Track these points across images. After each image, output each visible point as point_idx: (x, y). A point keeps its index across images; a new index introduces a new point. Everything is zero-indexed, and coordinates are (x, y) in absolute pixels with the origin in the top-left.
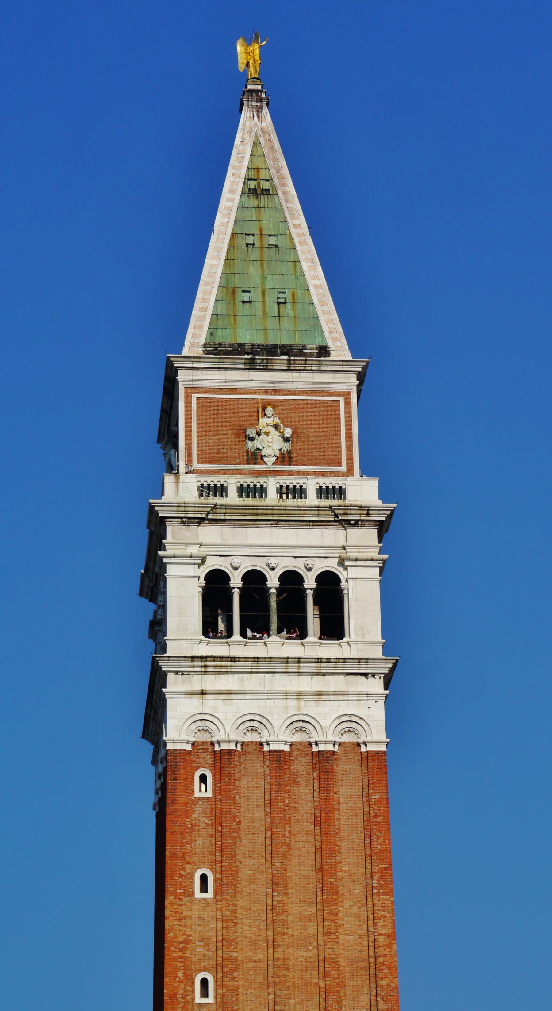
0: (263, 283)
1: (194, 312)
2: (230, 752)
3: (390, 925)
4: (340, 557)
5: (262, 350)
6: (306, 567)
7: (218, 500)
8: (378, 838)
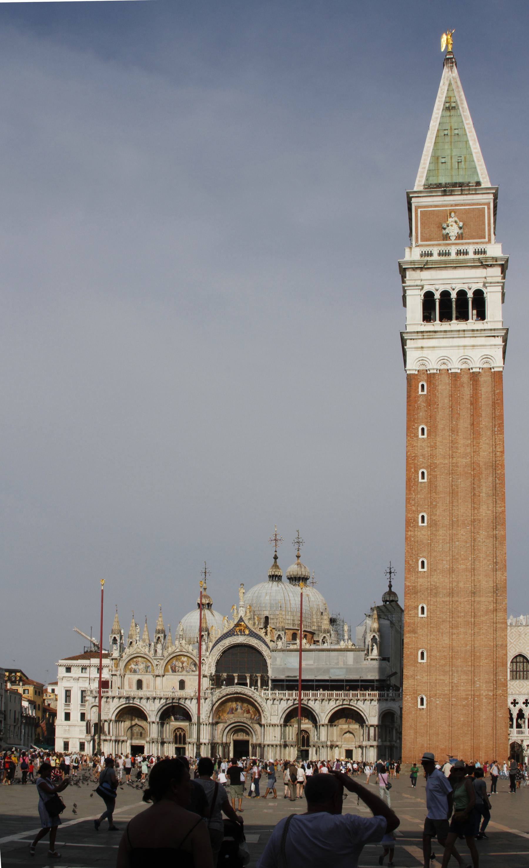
0: (451, 153)
1: (419, 170)
2: (434, 374)
3: (502, 447)
4: (484, 282)
5: (450, 186)
6: (468, 288)
7: (429, 258)
8: (498, 409)
